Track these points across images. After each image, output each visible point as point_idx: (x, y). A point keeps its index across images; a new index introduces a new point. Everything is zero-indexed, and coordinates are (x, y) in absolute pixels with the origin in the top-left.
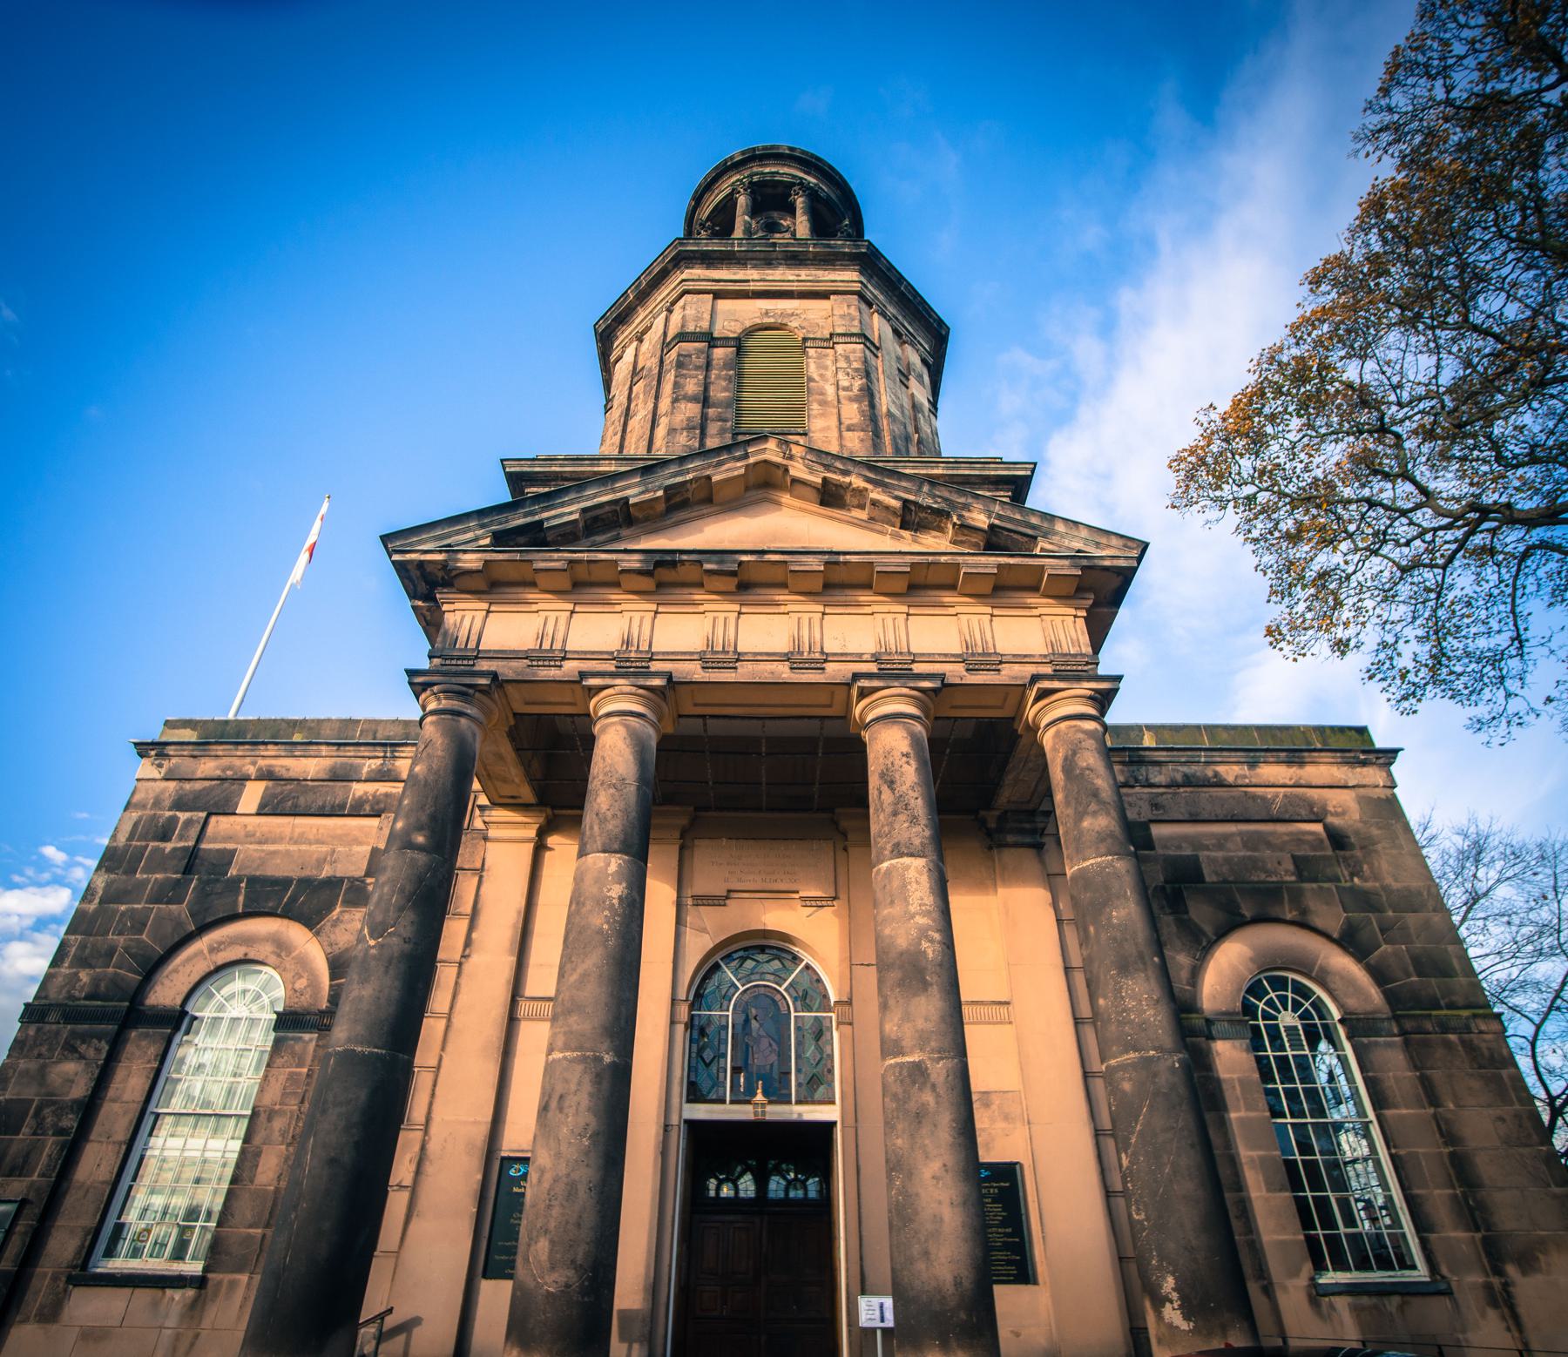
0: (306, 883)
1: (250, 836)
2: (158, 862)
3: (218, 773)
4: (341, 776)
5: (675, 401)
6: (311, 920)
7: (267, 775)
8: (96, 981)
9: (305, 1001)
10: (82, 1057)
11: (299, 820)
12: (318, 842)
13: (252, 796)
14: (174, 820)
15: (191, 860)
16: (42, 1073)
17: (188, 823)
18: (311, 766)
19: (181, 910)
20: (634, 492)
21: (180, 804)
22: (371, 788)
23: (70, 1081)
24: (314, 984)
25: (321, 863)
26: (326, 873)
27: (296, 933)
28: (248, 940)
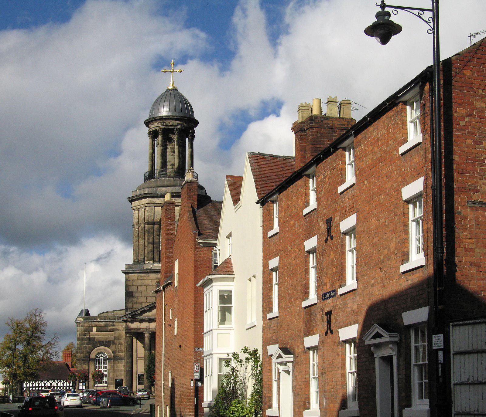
0: (106, 342)
1: (96, 335)
2: (85, 339)
3: (88, 326)
4: (107, 326)
5: (148, 244)
6: (108, 346)
7: (96, 326)
8: (84, 355)
9: (110, 357)
10: (86, 365)
11: (102, 332)
12: (107, 335)
13: (95, 329)
14: (85, 333)
15: (89, 339)
16: (82, 367)
17: (87, 333)
18: (102, 324)
19: (91, 346)
20: (146, 309)
21: (85, 331)
22: (111, 327)
23: (86, 367)
24: (110, 354)
25: (107, 339)
26: (108, 340)
27: (107, 348)
28: (100, 349)
